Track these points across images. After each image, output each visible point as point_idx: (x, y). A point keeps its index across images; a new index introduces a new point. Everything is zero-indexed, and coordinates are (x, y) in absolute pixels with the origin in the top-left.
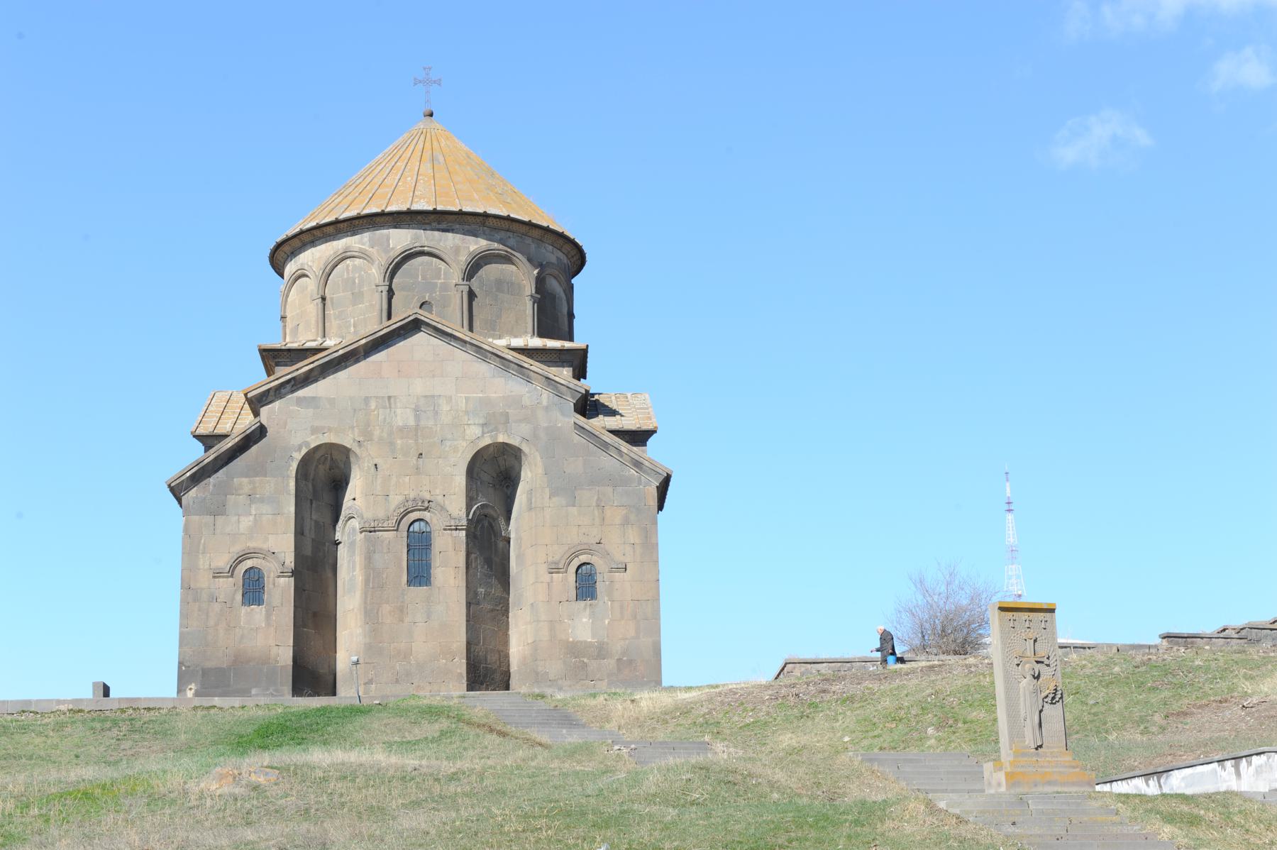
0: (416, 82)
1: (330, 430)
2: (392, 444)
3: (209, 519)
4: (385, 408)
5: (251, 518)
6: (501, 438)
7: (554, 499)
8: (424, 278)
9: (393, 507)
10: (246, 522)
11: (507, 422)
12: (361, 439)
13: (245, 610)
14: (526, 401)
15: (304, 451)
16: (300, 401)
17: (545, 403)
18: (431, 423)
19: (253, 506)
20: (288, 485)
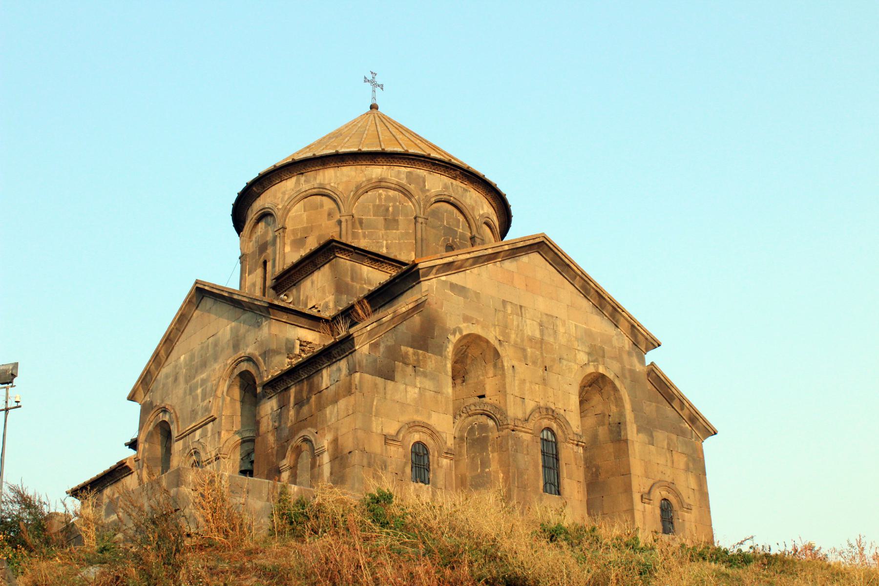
0: (366, 80)
1: (478, 322)
2: (524, 350)
3: (380, 381)
4: (517, 315)
5: (417, 390)
6: (601, 370)
7: (640, 435)
8: (448, 223)
9: (528, 411)
10: (413, 393)
11: (604, 357)
12: (501, 338)
13: (413, 486)
14: (615, 343)
15: (458, 336)
16: (453, 287)
17: (627, 347)
18: (551, 340)
19: (418, 379)
20: (445, 365)
